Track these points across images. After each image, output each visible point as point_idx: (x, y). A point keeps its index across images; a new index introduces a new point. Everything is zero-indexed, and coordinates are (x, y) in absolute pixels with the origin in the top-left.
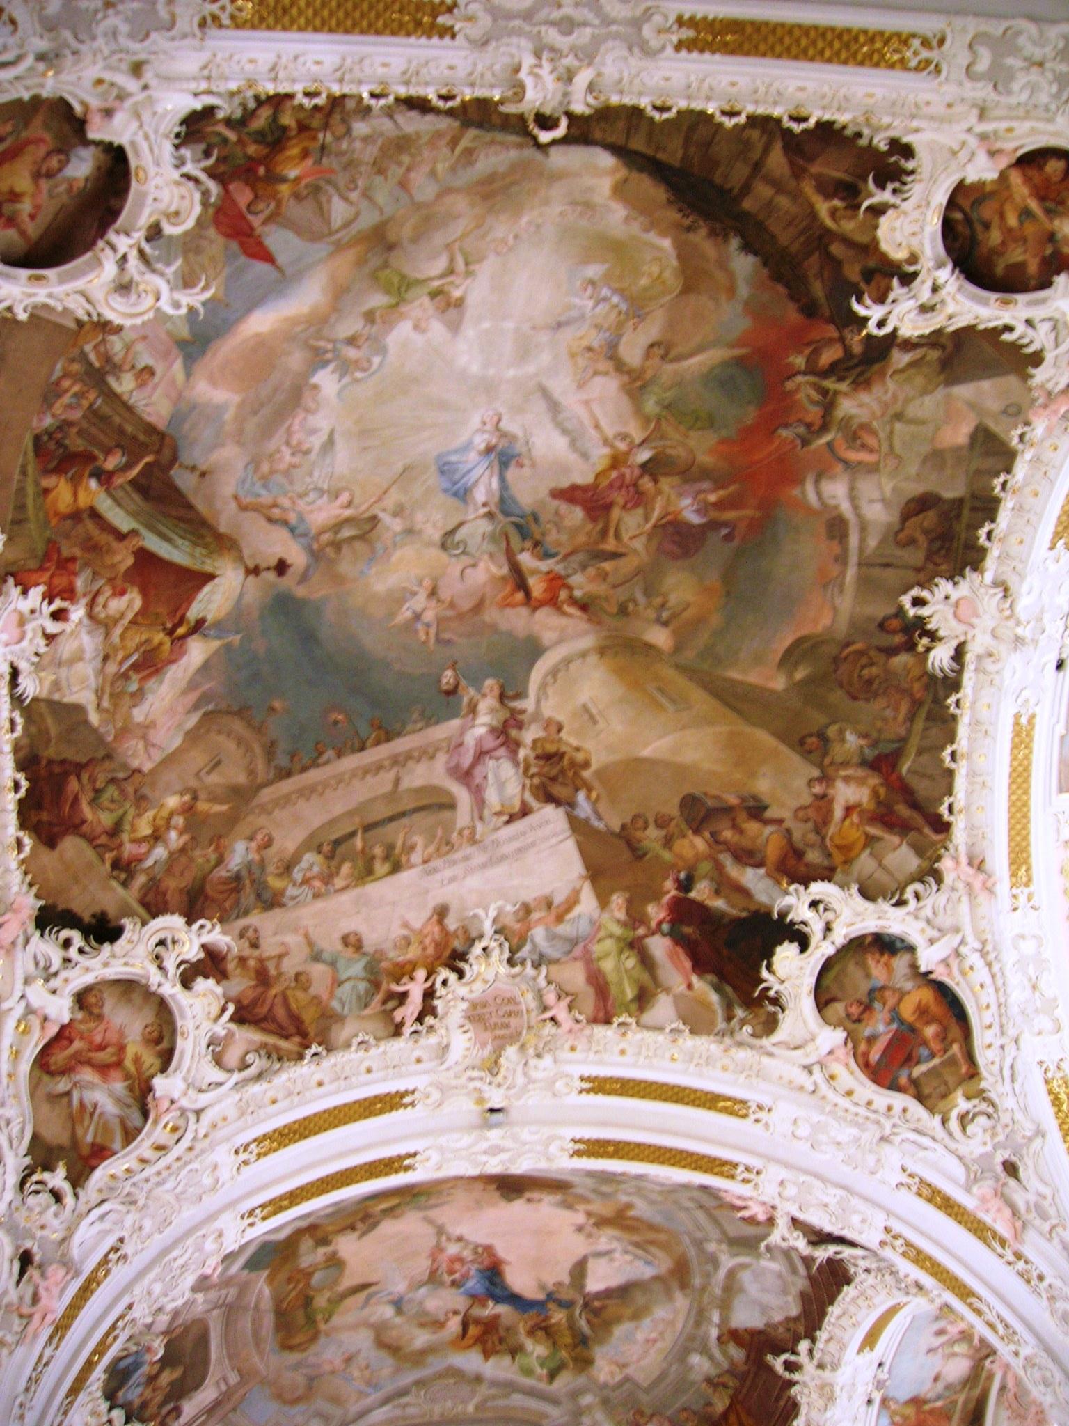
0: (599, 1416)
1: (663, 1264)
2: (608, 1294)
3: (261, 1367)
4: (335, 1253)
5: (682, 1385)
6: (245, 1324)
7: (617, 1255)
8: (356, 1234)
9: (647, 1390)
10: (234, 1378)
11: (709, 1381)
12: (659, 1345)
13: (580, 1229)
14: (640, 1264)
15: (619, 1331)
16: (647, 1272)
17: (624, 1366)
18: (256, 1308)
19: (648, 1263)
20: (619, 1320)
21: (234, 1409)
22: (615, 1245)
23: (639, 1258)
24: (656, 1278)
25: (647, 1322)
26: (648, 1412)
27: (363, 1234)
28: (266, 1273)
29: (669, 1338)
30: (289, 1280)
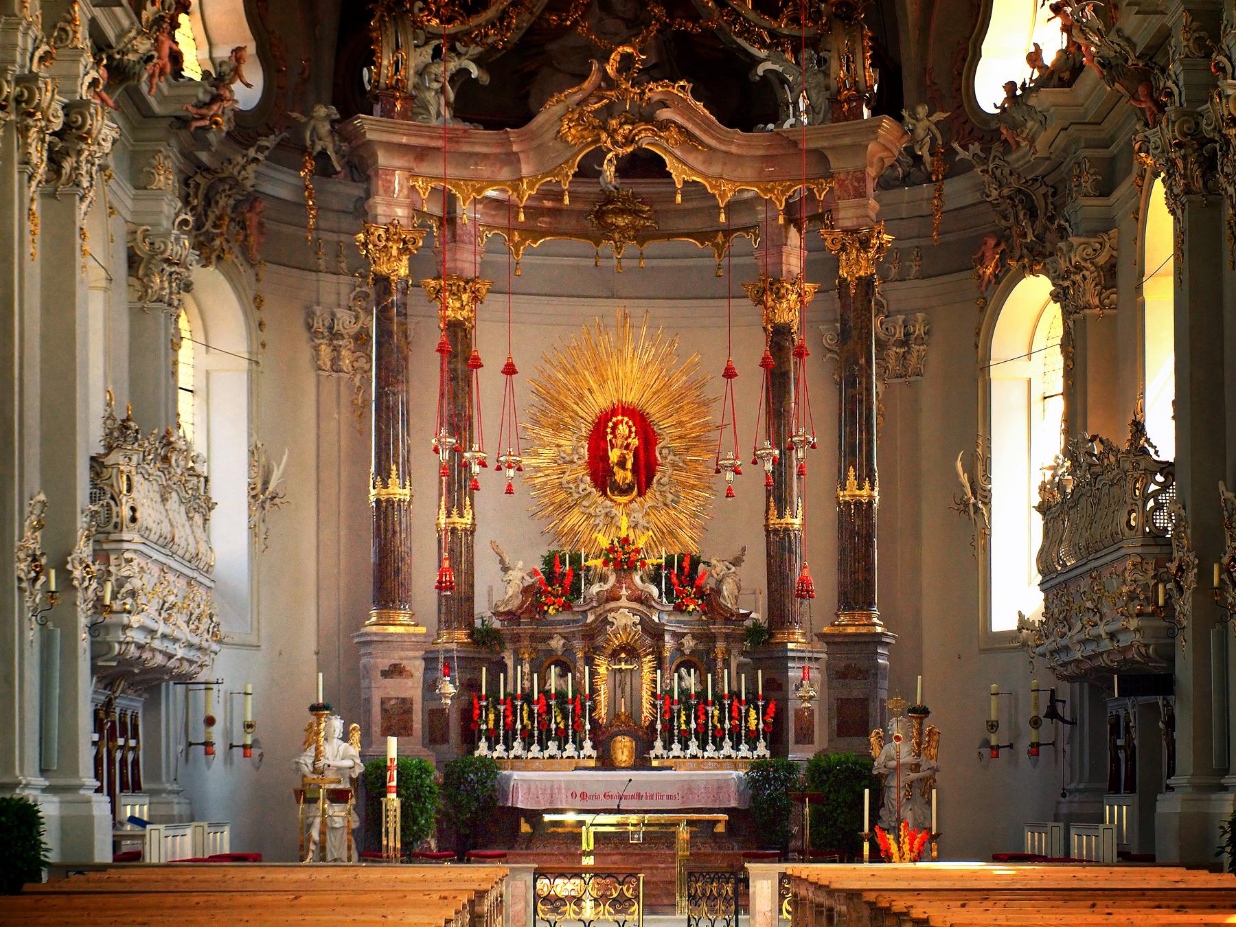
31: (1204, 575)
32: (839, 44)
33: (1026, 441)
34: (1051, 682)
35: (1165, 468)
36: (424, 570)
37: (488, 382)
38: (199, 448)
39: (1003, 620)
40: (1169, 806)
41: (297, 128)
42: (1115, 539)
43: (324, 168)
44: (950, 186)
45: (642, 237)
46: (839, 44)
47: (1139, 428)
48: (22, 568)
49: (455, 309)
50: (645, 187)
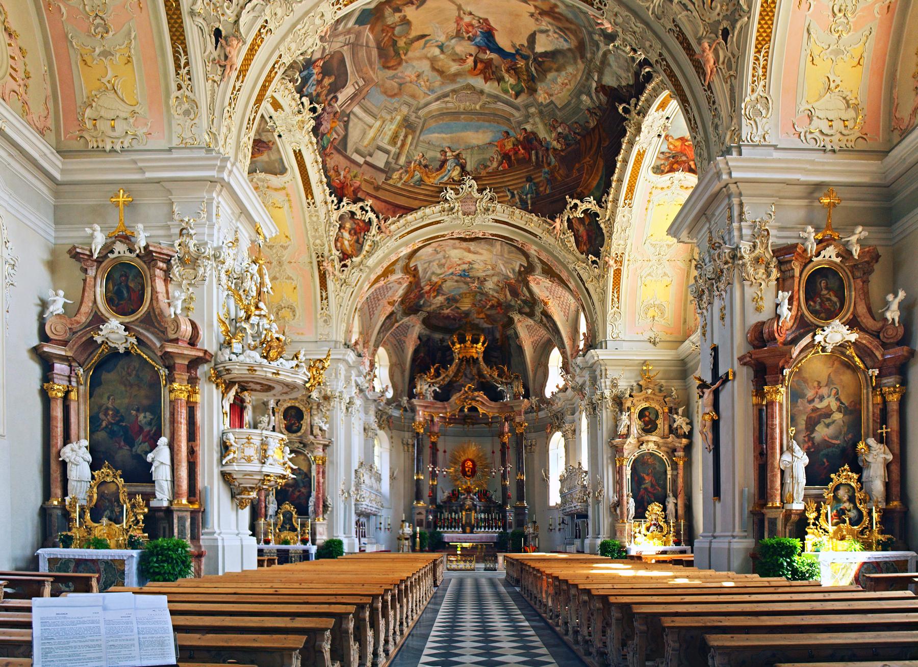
0: (537, 120)
1: (573, 43)
2: (545, 54)
3: (374, 77)
4: (405, 16)
5: (577, 110)
6: (363, 53)
7: (550, 33)
8: (415, 7)
9: (560, 110)
10: (361, 83)
11: (588, 110)
12: (568, 87)
13: (532, 15)
14: (562, 40)
15: (550, 76)
16: (565, 46)
17: (551, 95)
18: (367, 46)
19: (566, 41)
20: (550, 70)
21: (364, 98)
22: (550, 27)
23: (562, 37)
24: (569, 50)
25: (564, 73)
26: (559, 121)
27: (418, 8)
28: (369, 26)
29: (573, 84)
30: (383, 31)
31: (594, 494)
32: (515, 383)
33: (557, 467)
34: (562, 516)
35: (586, 472)
36: (426, 492)
37: (440, 454)
38: (379, 468)
39: (552, 503)
40: (587, 541)
41: (400, 402)
42: (575, 486)
43: (405, 410)
44: (540, 413)
45: (473, 424)
46: (515, 383)
47: (580, 464)
48: (340, 492)
49: (433, 439)
50: (474, 414)
